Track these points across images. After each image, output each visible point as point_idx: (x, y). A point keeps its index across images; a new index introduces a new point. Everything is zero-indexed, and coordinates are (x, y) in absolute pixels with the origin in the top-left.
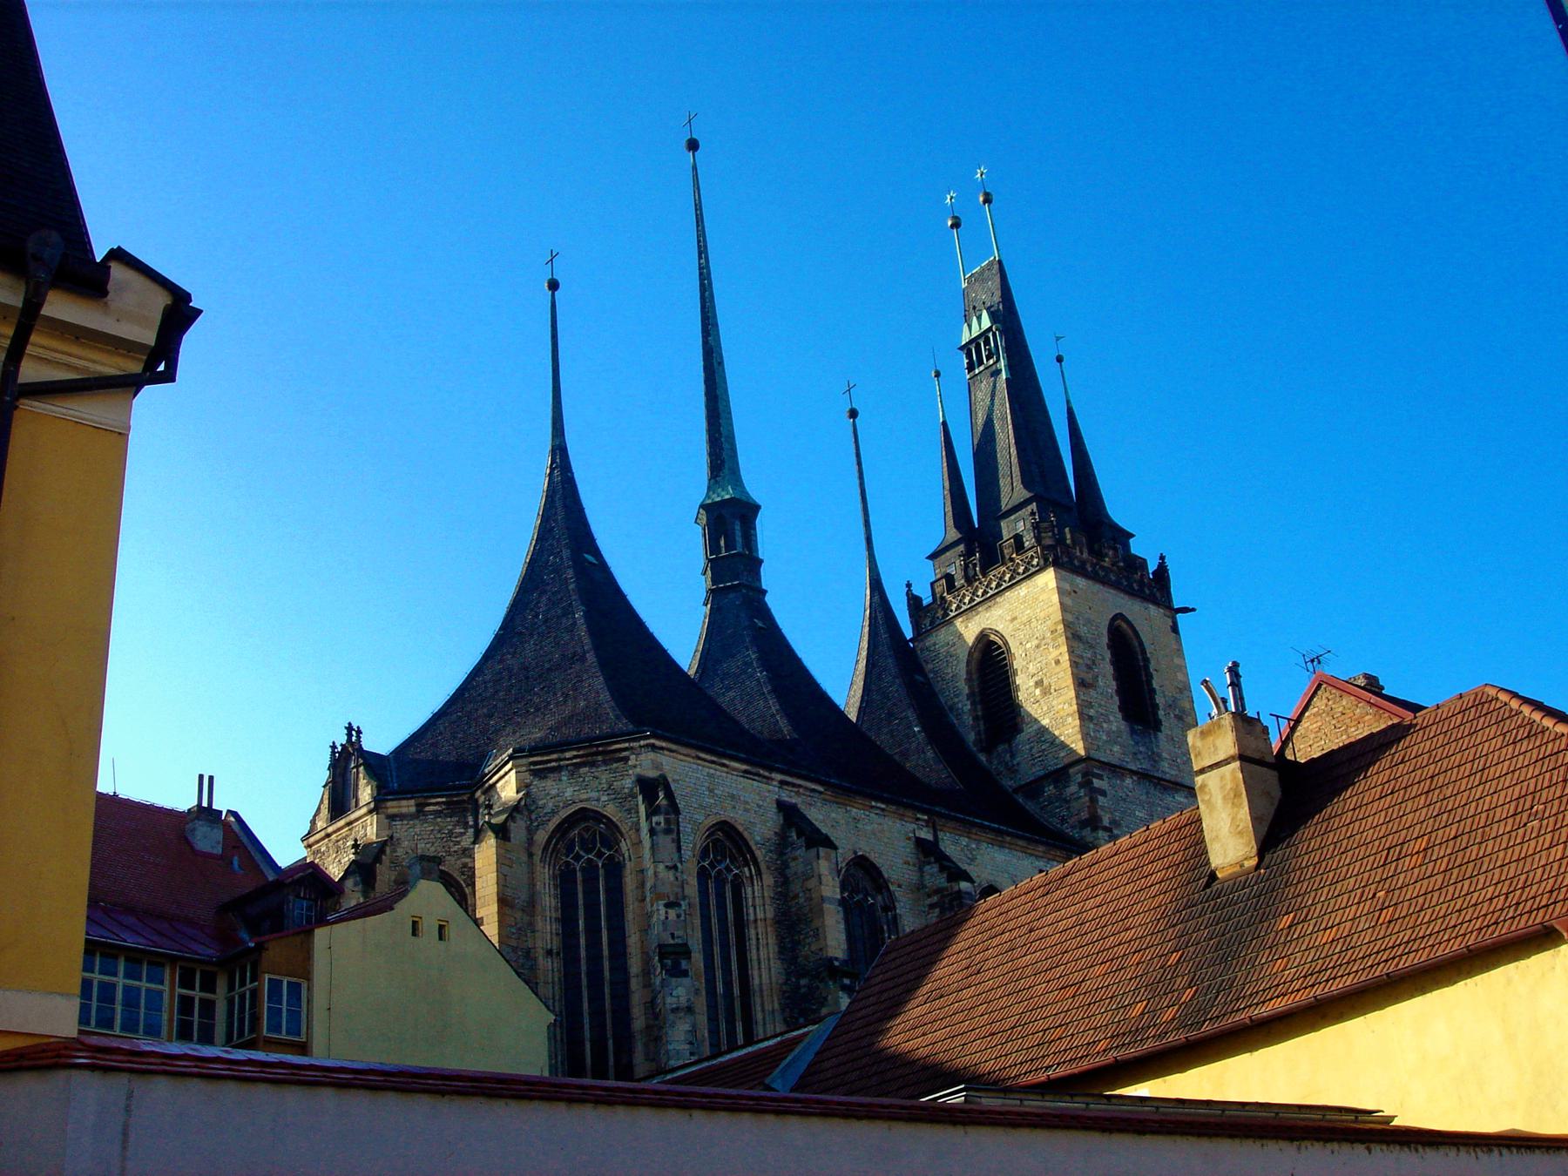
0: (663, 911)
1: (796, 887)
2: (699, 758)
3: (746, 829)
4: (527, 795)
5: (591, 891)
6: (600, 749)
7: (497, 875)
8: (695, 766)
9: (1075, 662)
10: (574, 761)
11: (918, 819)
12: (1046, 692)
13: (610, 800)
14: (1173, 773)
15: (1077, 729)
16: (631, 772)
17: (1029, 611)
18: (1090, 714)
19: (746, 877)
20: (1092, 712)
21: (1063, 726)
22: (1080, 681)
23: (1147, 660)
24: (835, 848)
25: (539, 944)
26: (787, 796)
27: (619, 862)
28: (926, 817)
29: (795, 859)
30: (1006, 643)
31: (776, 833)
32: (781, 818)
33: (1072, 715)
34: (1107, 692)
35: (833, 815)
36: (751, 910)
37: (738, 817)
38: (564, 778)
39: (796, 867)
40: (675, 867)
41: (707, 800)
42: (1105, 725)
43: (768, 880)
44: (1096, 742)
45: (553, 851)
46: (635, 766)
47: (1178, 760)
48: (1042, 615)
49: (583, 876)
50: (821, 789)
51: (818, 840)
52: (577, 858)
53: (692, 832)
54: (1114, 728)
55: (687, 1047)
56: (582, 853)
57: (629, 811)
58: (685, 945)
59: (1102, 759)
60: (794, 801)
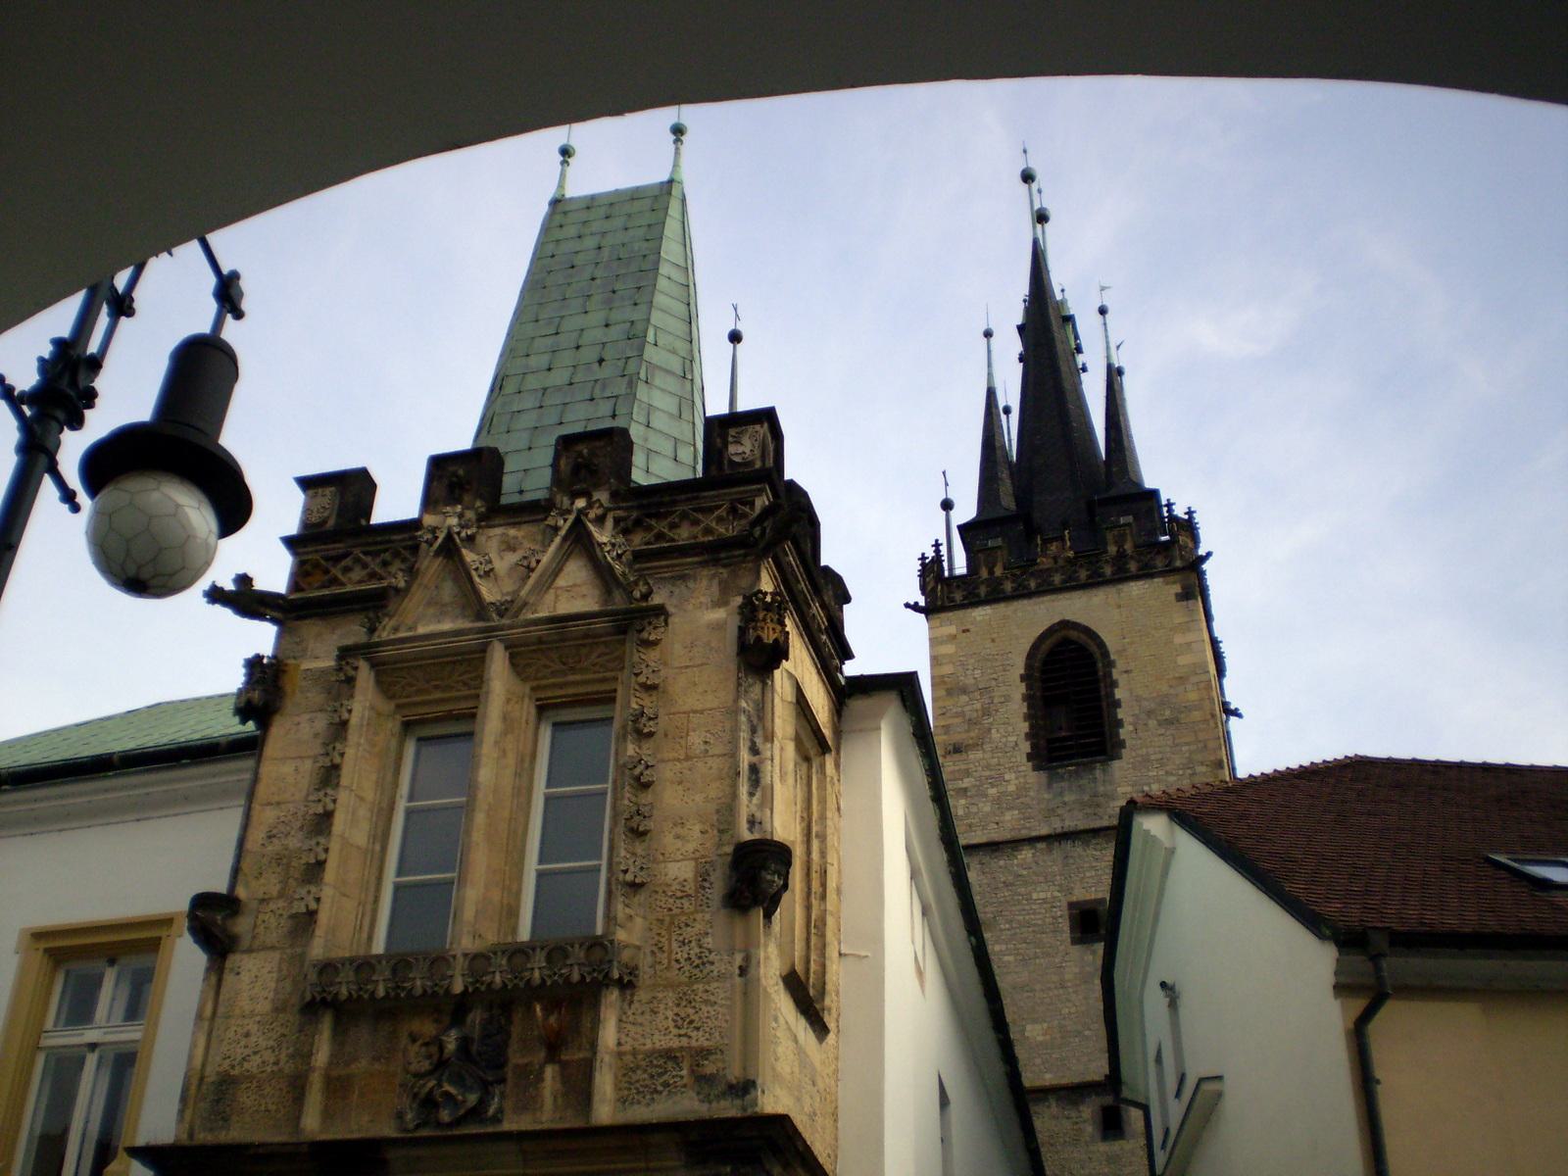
9: (943, 726)
20: (967, 783)
23: (1111, 664)
42: (992, 791)
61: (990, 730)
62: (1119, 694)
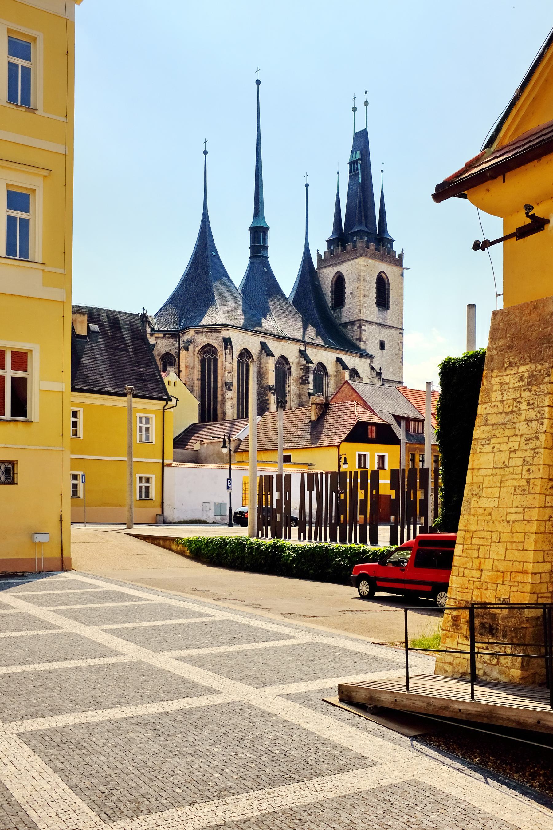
25: (195, 377)
26: (263, 340)
52: (206, 356)
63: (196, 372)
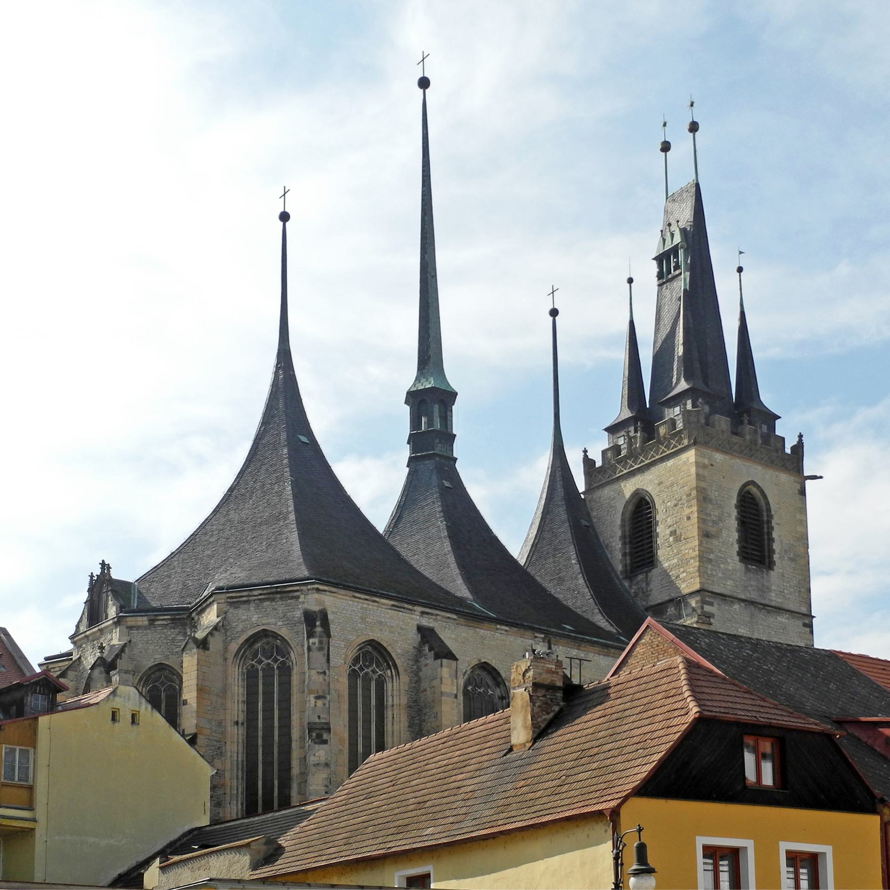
0: (313, 701)
1: (424, 685)
2: (355, 597)
3: (390, 645)
4: (224, 619)
5: (268, 685)
6: (279, 590)
7: (197, 673)
8: (351, 603)
10: (260, 597)
11: (536, 637)
12: (678, 539)
13: (284, 625)
14: (780, 600)
15: (696, 568)
16: (300, 606)
17: (672, 478)
18: (710, 557)
19: (388, 677)
20: (712, 556)
21: (687, 565)
22: (705, 533)
24: (455, 659)
26: (426, 622)
27: (289, 667)
28: (543, 636)
29: (426, 665)
30: (653, 501)
31: (414, 648)
32: (419, 635)
33: (693, 558)
34: (728, 541)
35: (464, 635)
36: (390, 699)
37: (383, 637)
38: (252, 609)
39: (425, 672)
40: (324, 673)
41: (359, 625)
42: (722, 566)
43: (405, 678)
44: (712, 579)
45: (242, 656)
46: (303, 603)
47: (785, 591)
48: (681, 482)
49: (263, 674)
50: (455, 617)
51: (444, 654)
52: (260, 662)
53: (345, 647)
54: (730, 568)
55: (324, 788)
56: (264, 659)
57: (297, 632)
58: (328, 724)
59: (714, 591)
60: (431, 625)
61: (721, 529)
62: (775, 535)
63: (229, 705)
